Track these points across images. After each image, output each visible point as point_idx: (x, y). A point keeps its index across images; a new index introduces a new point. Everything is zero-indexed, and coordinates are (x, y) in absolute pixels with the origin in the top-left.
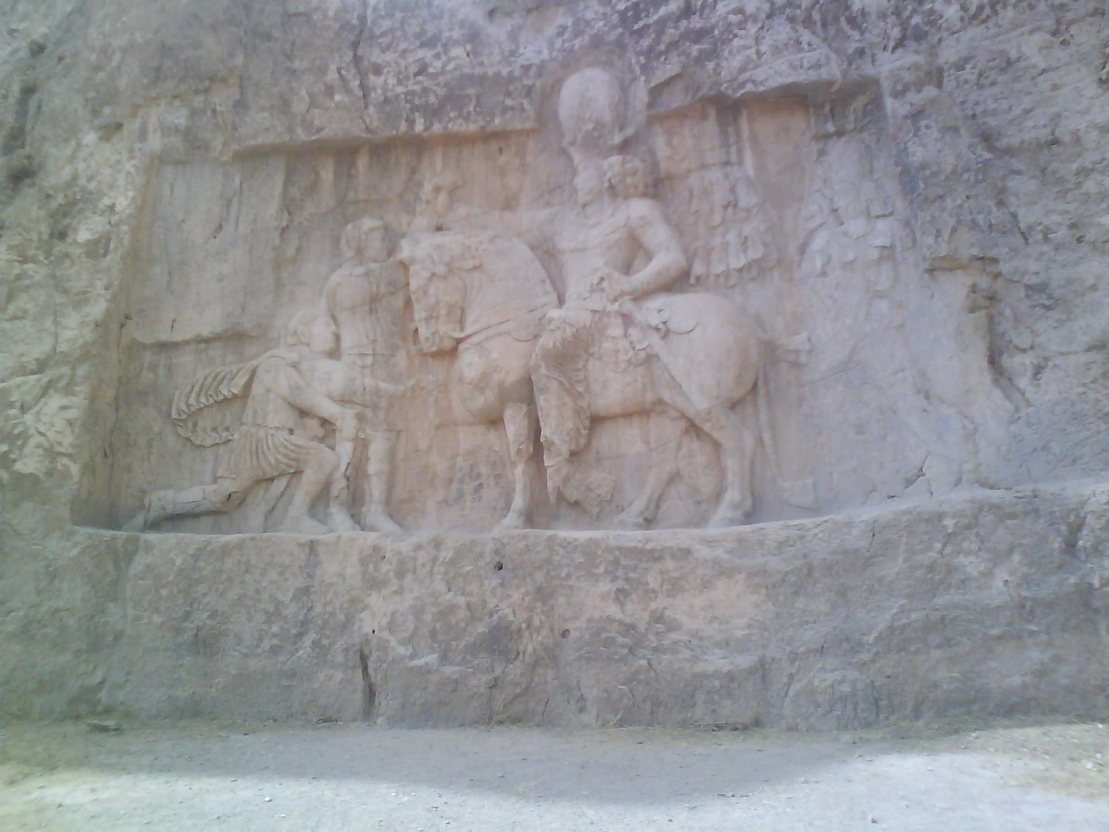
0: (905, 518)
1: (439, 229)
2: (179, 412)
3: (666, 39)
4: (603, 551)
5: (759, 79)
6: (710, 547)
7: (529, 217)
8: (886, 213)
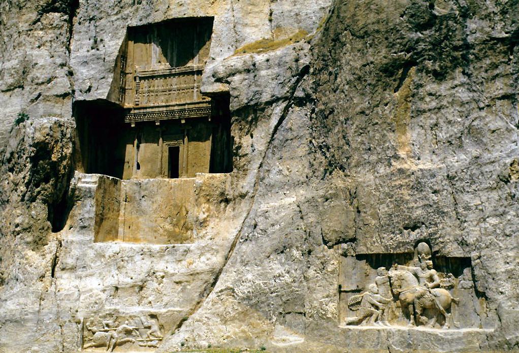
1: (396, 270)
7: (411, 268)
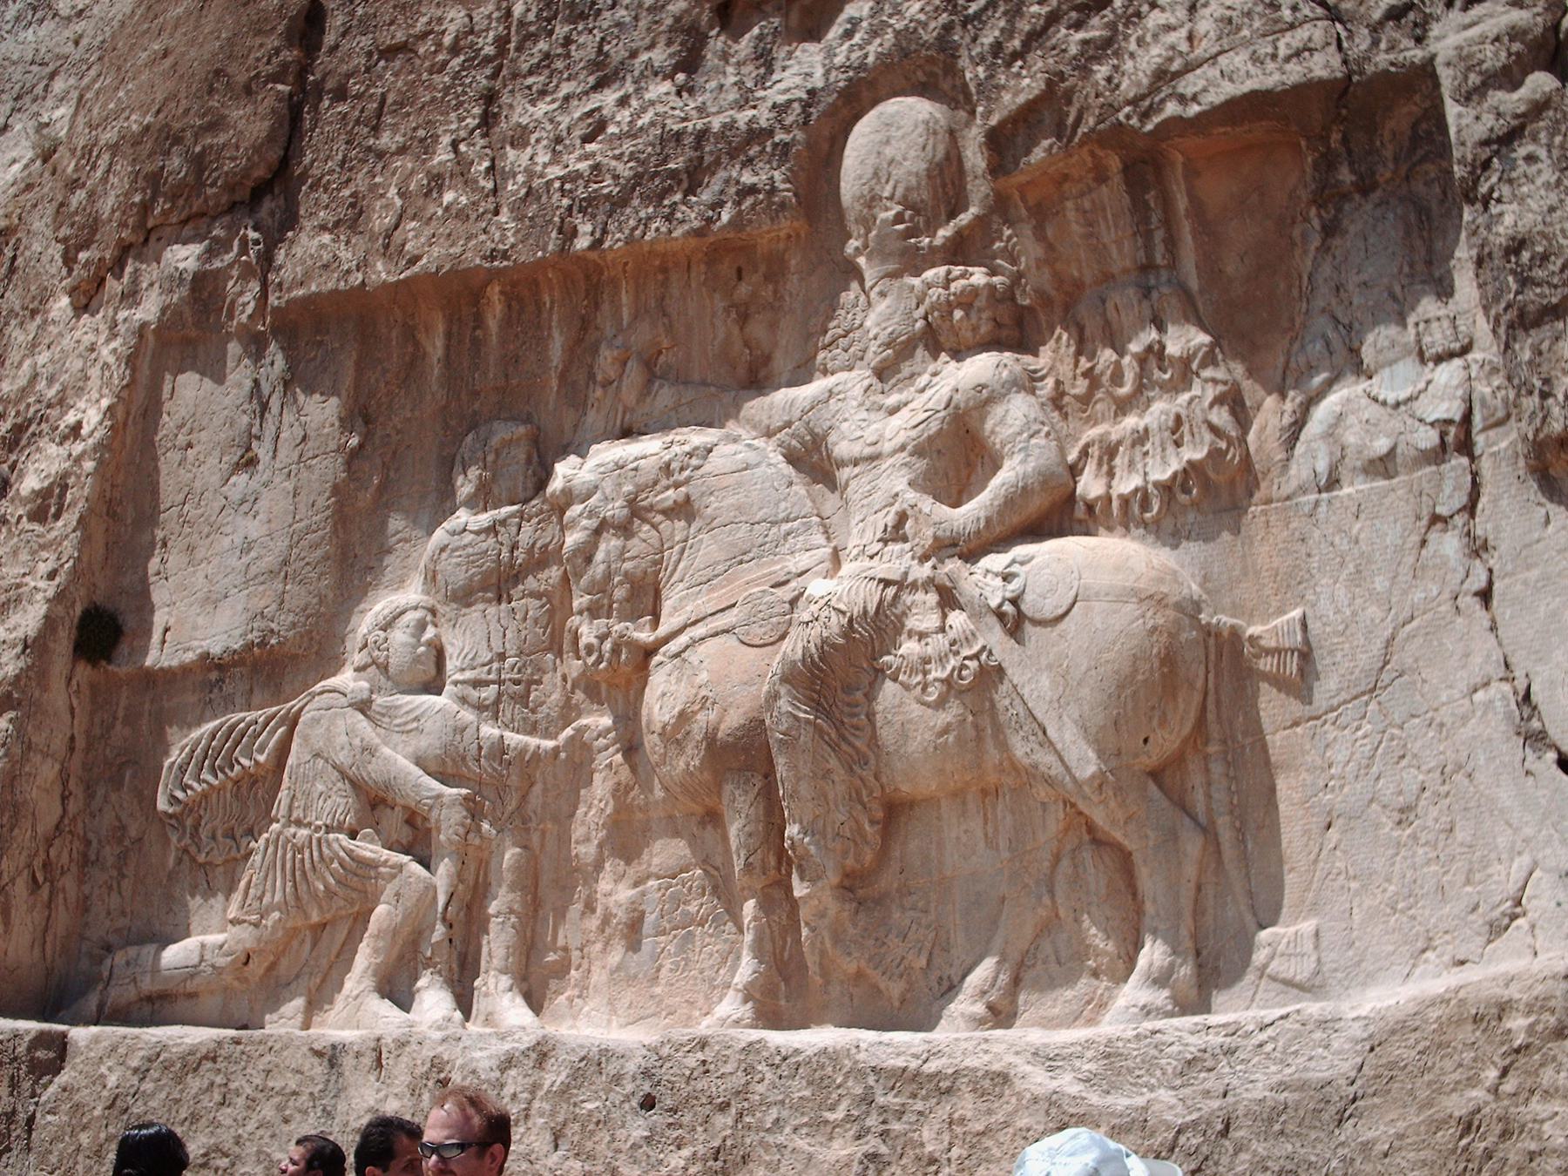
0: (1433, 1014)
2: (173, 800)
3: (1024, 26)
4: (847, 1076)
5: (1189, 91)
6: (1051, 1069)
8: (1456, 346)
